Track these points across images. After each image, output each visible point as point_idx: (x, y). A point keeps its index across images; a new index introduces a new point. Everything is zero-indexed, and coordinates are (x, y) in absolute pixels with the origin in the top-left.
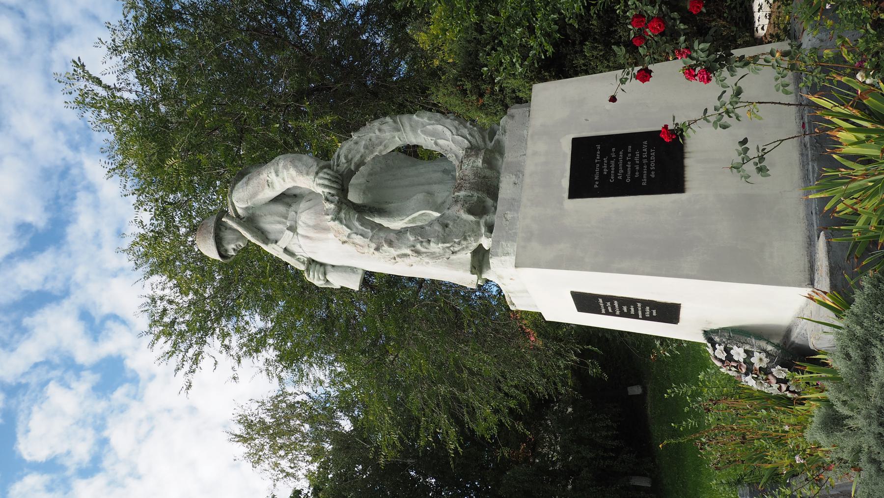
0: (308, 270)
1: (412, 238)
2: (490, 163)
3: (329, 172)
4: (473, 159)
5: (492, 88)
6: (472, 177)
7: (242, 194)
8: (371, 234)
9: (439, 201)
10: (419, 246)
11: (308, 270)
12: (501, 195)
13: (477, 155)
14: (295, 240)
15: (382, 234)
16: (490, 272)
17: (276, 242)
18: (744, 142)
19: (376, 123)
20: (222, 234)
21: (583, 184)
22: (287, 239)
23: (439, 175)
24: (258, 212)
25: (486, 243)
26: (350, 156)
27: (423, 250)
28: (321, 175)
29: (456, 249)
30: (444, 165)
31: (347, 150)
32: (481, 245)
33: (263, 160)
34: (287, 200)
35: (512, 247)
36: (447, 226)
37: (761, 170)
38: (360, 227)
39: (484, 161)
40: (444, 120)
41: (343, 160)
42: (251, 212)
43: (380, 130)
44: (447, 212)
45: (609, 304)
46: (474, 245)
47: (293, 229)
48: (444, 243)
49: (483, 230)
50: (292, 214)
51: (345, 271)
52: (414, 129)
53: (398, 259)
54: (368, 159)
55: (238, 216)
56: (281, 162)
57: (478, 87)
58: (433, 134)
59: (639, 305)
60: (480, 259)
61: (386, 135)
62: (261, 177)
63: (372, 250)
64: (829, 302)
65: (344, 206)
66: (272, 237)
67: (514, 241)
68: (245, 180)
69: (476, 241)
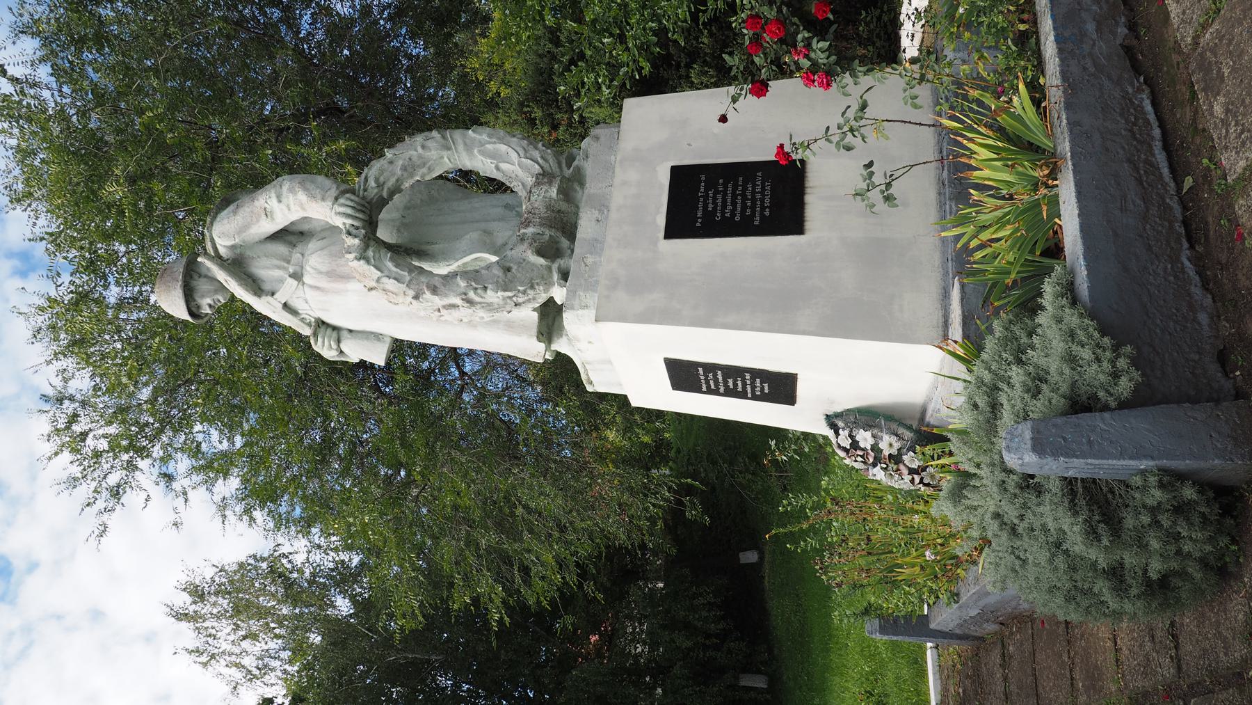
0: (315, 334)
1: (463, 284)
3: (353, 197)
4: (545, 188)
5: (570, 119)
6: (543, 210)
7: (228, 226)
8: (408, 278)
9: (500, 242)
10: (471, 294)
11: (315, 334)
12: (580, 234)
13: (550, 183)
14: (300, 292)
15: (423, 279)
16: (564, 339)
17: (273, 294)
18: (870, 164)
19: (419, 138)
20: (194, 283)
21: (682, 222)
22: (288, 291)
23: (500, 211)
24: (248, 253)
26: (382, 179)
27: (477, 299)
28: (342, 201)
29: (520, 300)
30: (507, 198)
32: (551, 300)
33: (258, 182)
34: (291, 238)
35: (591, 299)
36: (509, 270)
37: (888, 198)
38: (394, 269)
39: (559, 191)
40: (508, 138)
41: (372, 183)
42: (238, 251)
43: (423, 147)
44: (509, 253)
45: (711, 375)
46: (543, 298)
47: (298, 276)
48: (505, 290)
49: (556, 277)
50: (296, 256)
51: (367, 338)
52: (469, 148)
53: (443, 312)
54: (407, 185)
55: (220, 257)
56: (286, 183)
57: (550, 115)
59: (748, 376)
60: (550, 317)
61: (434, 154)
62: (256, 203)
63: (409, 299)
64: (960, 352)
65: (372, 243)
66: (266, 287)
67: (595, 291)
68: (232, 207)
69: (546, 291)
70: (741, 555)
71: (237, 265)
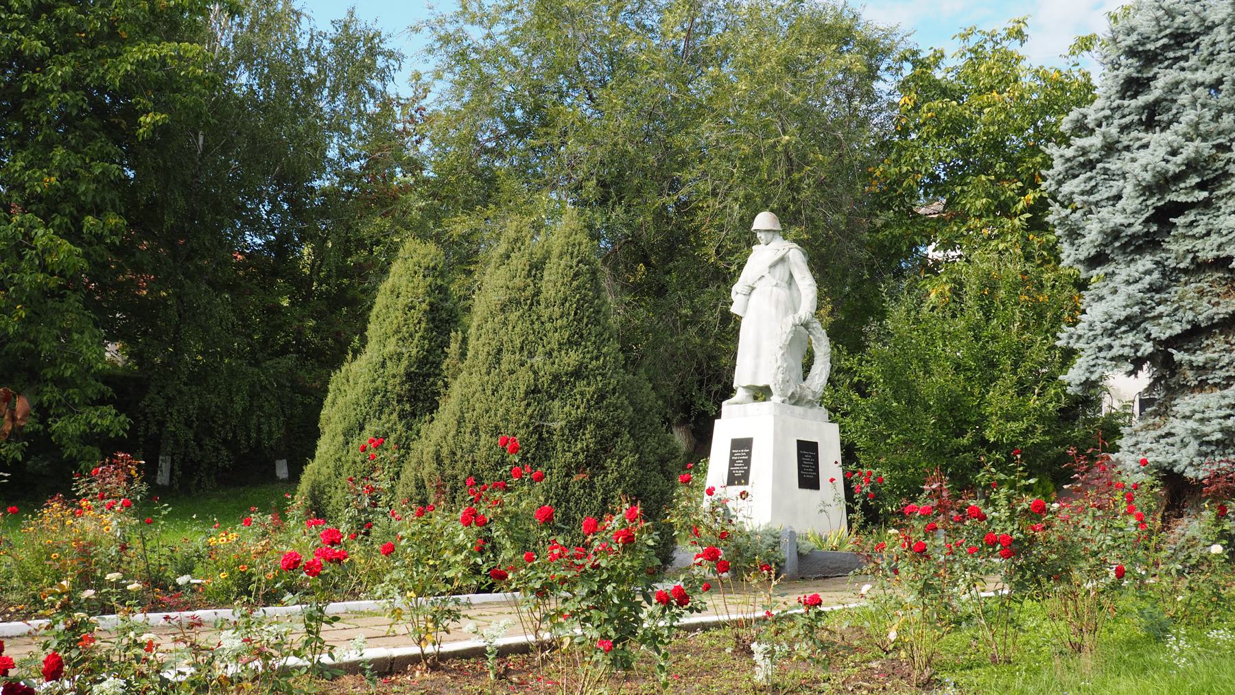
2: (809, 402)
22: (770, 280)
25: (776, 398)
31: (817, 325)
47: (776, 285)
50: (784, 284)
58: (821, 373)
70: (285, 461)
71: (782, 260)
